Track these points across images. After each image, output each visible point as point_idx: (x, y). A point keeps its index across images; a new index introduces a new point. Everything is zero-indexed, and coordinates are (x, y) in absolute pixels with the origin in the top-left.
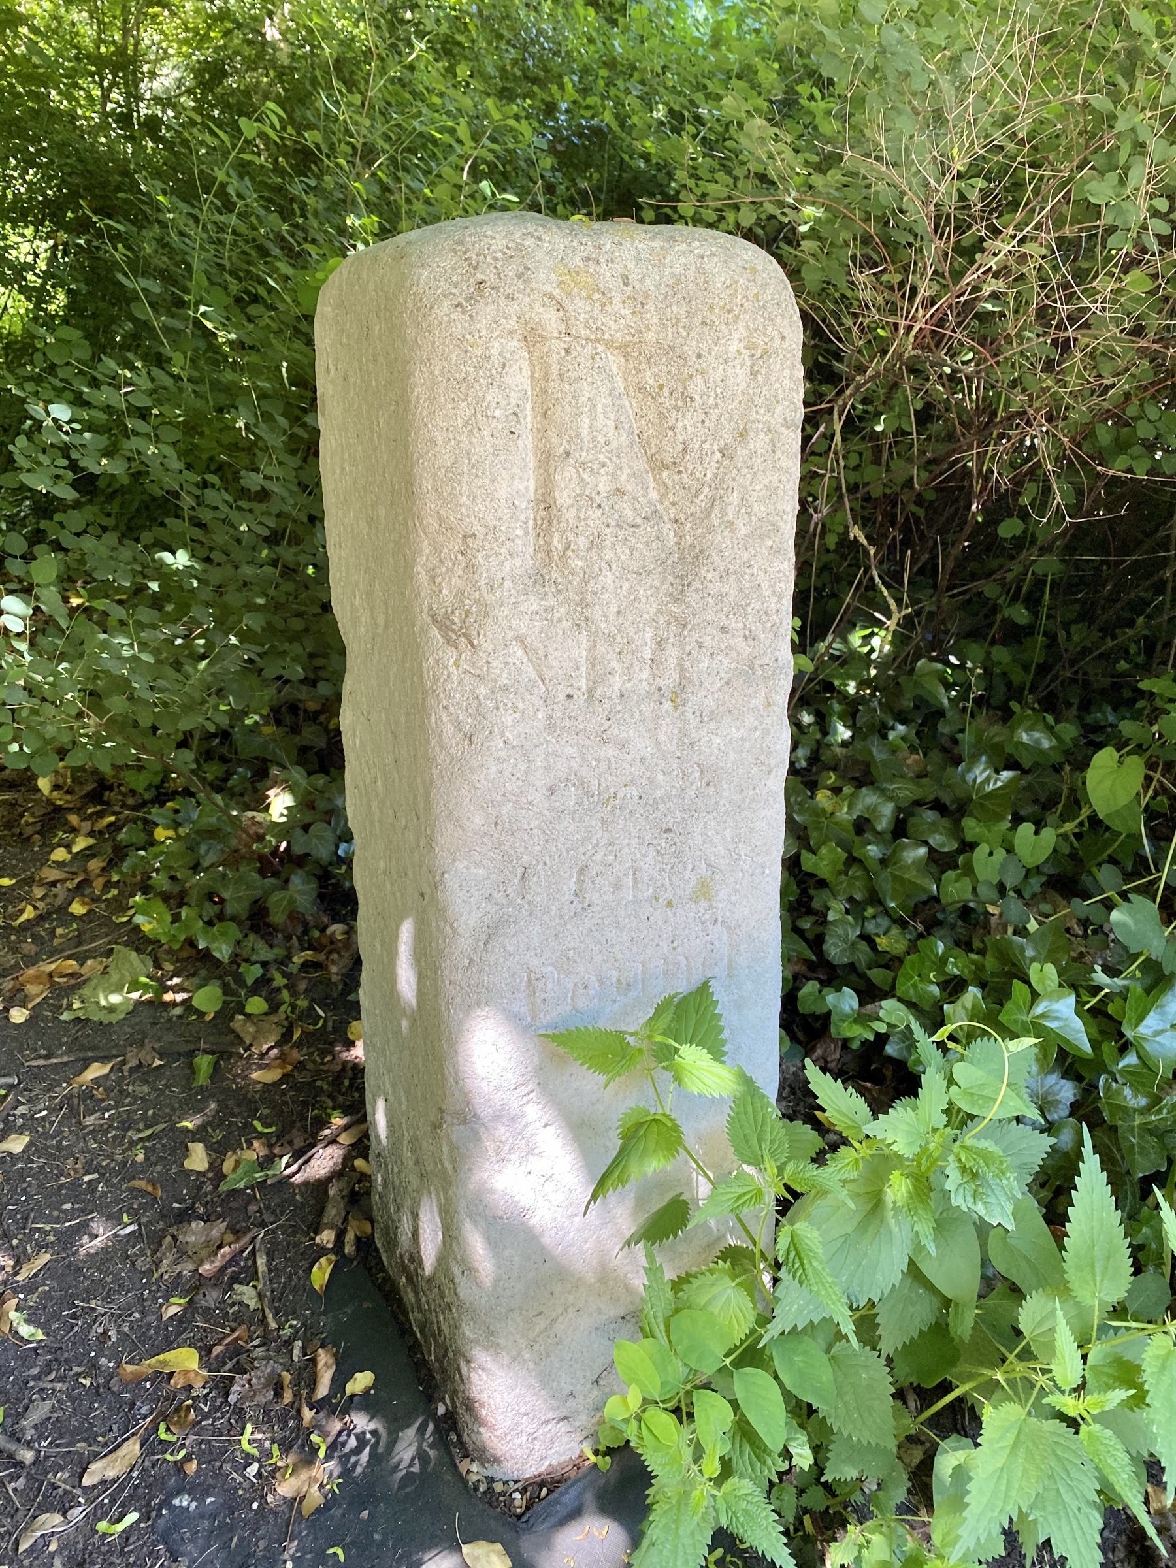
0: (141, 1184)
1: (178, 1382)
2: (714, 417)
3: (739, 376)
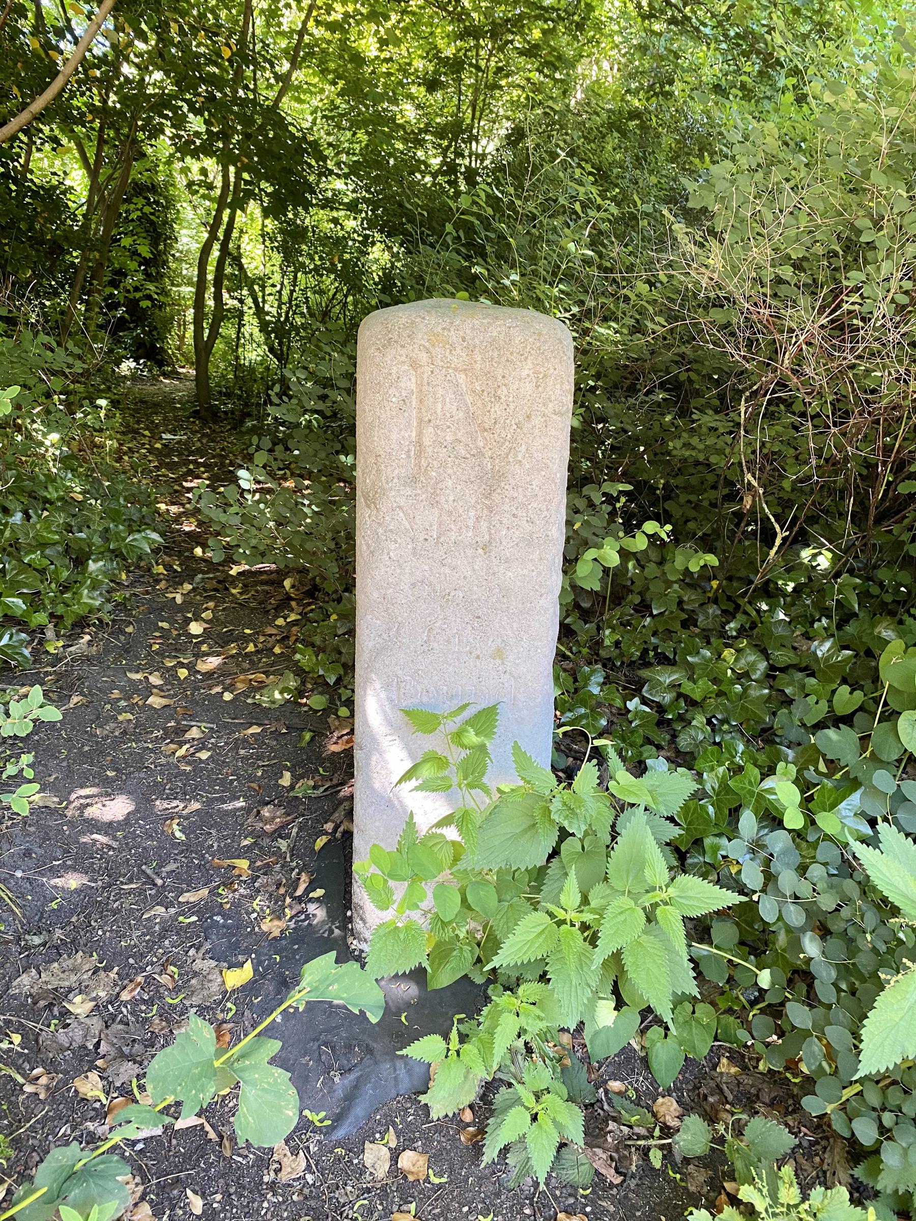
0: (254, 785)
1: (236, 872)
2: (512, 408)
3: (528, 388)
